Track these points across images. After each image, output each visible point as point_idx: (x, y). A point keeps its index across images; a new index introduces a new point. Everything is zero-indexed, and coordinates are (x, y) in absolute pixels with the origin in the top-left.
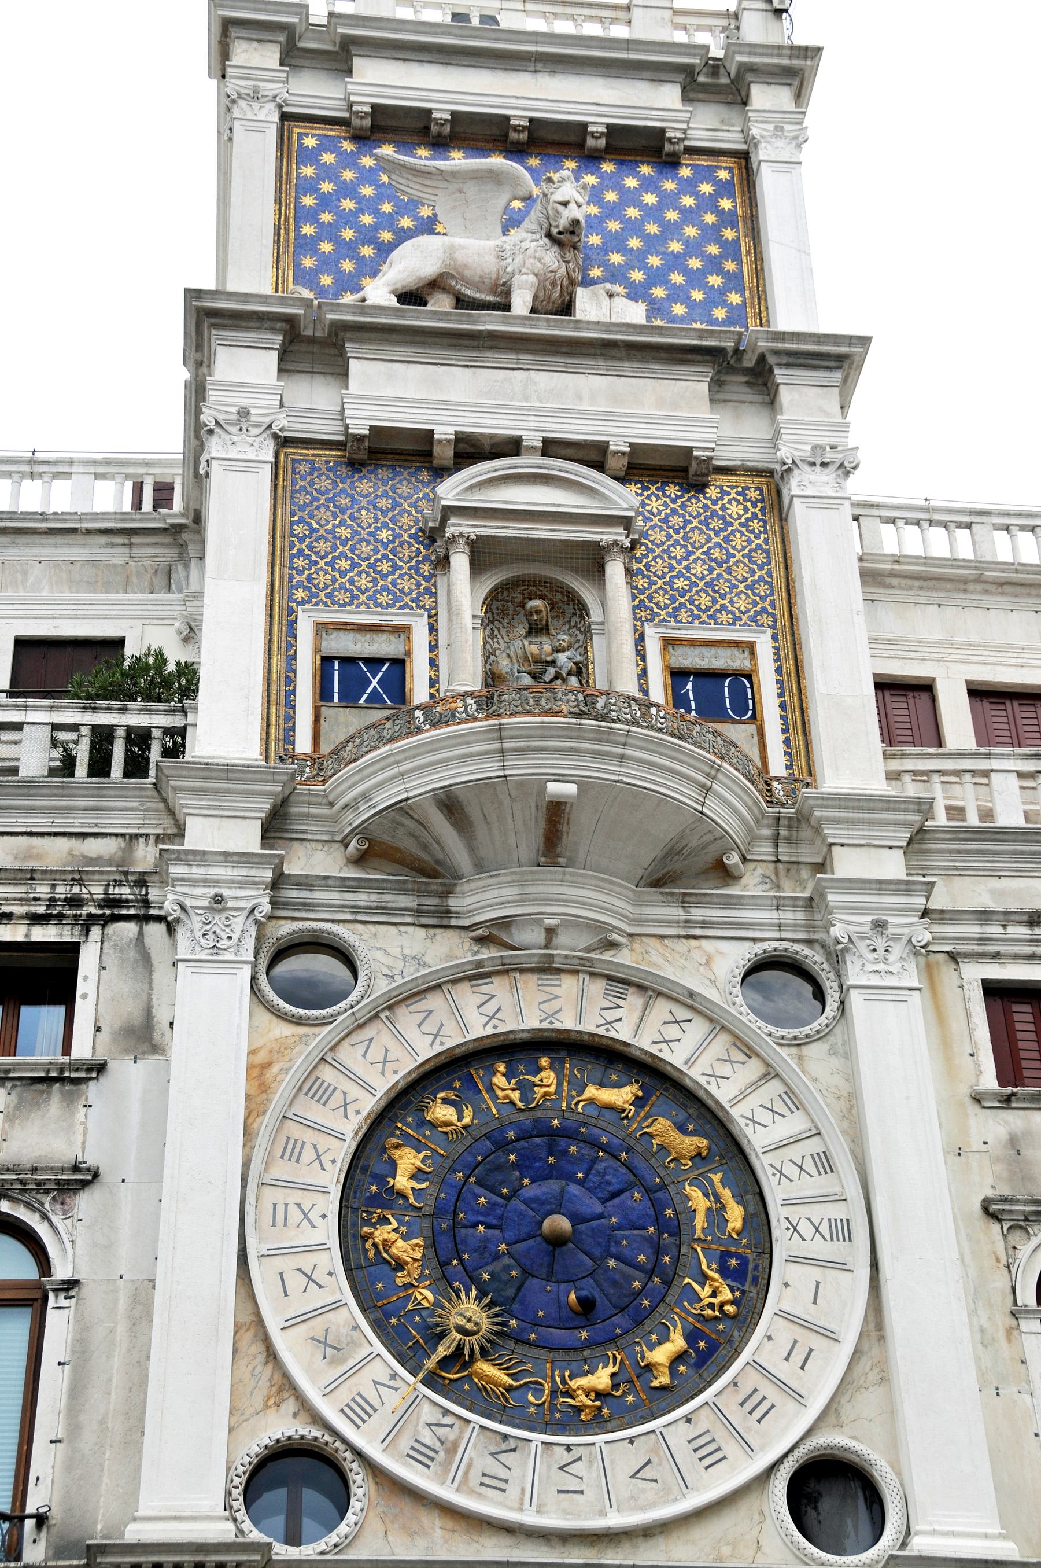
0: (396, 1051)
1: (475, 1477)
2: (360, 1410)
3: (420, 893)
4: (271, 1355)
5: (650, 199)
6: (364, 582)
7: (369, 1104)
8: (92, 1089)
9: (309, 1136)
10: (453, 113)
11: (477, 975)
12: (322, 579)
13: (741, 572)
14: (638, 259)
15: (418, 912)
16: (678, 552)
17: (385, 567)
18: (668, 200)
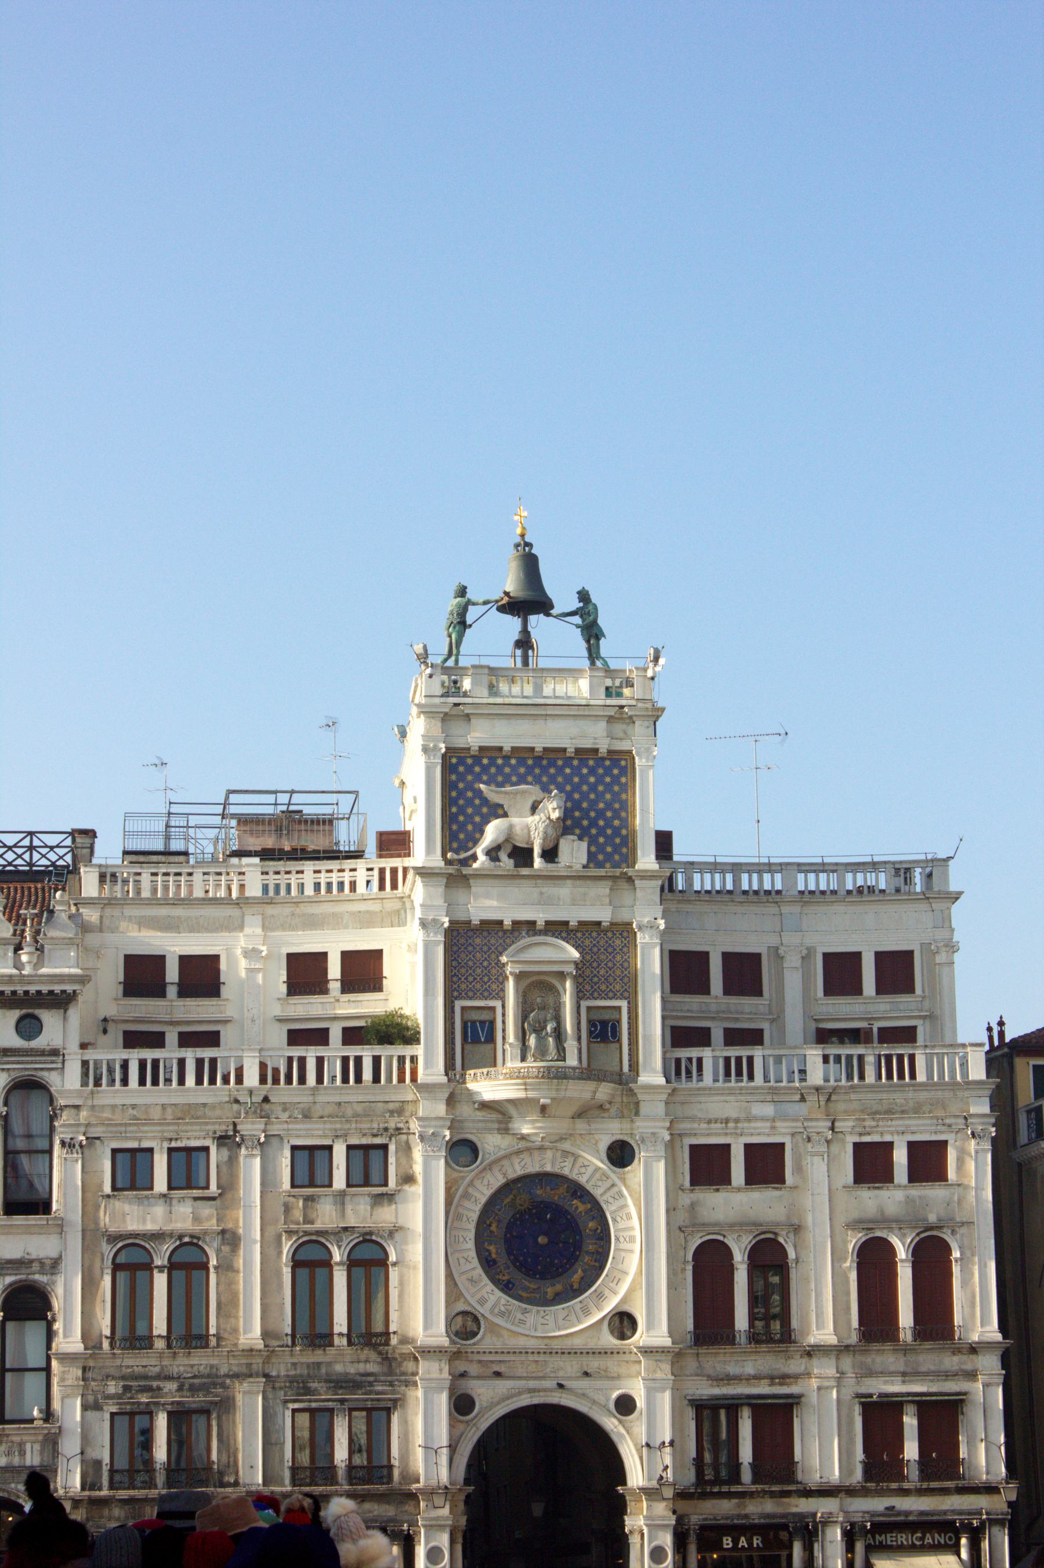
0: (492, 1180)
1: (517, 1321)
2: (482, 1302)
3: (500, 1122)
4: (456, 1284)
5: (592, 780)
6: (478, 986)
7: (483, 1200)
8: (397, 1198)
9: (465, 1212)
10: (513, 748)
11: (518, 1152)
12: (463, 986)
13: (618, 972)
14: (586, 814)
15: (498, 1129)
16: (595, 964)
17: (486, 979)
18: (600, 780)
